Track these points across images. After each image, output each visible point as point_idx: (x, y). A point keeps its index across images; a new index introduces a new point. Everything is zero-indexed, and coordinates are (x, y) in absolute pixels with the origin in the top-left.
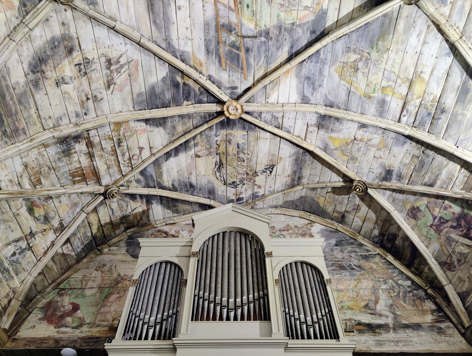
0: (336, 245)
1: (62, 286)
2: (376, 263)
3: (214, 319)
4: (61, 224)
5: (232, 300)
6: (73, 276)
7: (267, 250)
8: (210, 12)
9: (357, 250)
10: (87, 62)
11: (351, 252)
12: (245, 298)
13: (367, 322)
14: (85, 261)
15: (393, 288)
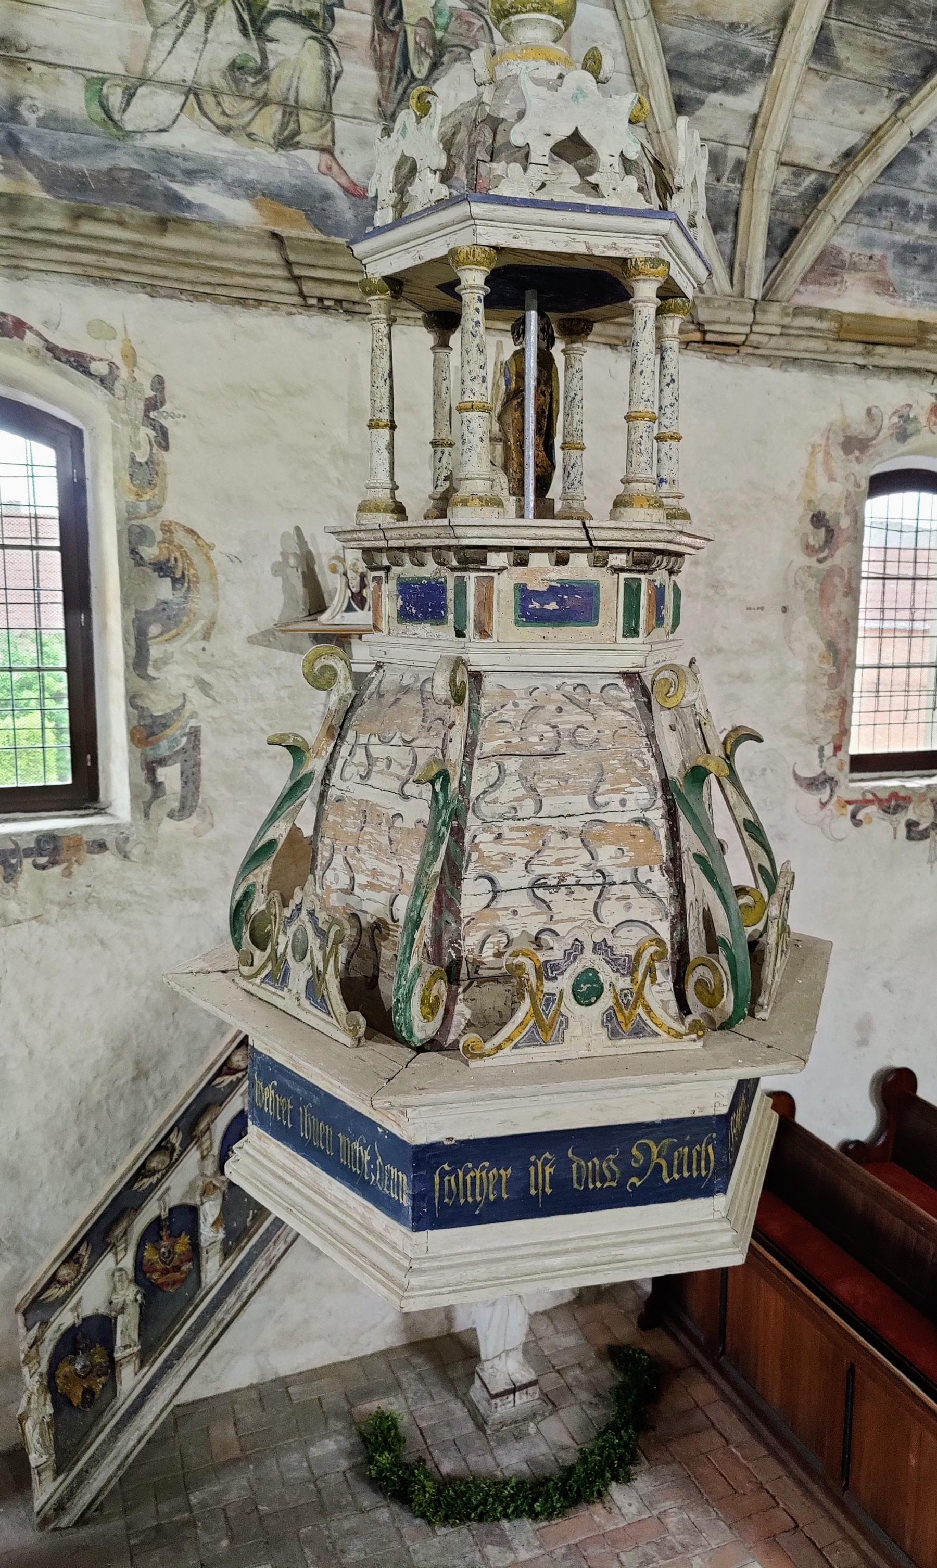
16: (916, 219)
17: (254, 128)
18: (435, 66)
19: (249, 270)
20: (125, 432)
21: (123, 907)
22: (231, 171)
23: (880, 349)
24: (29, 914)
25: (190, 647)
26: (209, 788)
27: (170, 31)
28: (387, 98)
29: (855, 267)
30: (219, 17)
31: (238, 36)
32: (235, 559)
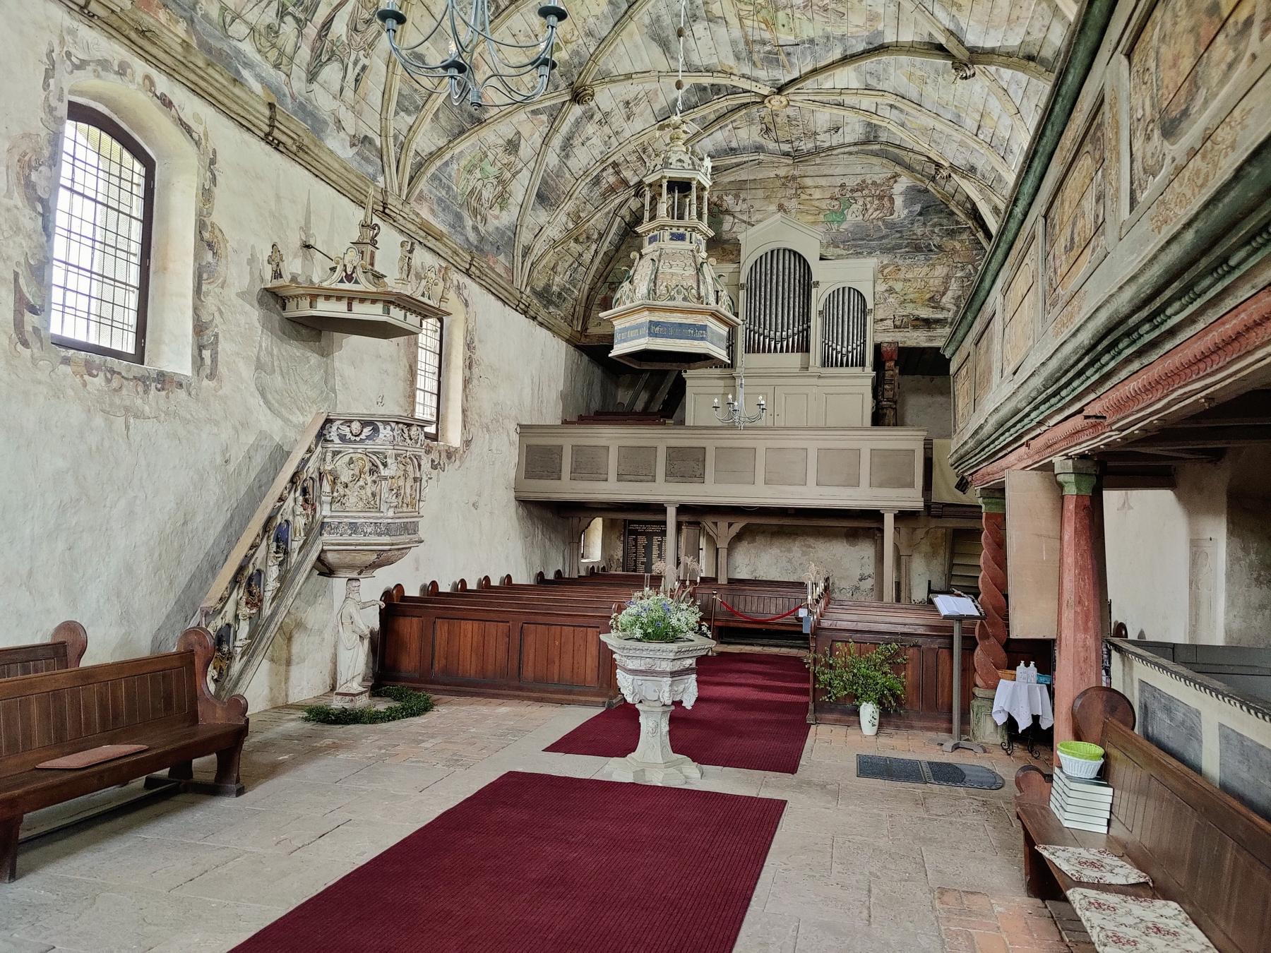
0: (920, 214)
1: (610, 279)
2: (962, 241)
3: (764, 351)
4: (599, 233)
5: (778, 334)
6: (617, 267)
7: (814, 279)
8: (736, 33)
9: (945, 221)
10: (606, 115)
11: (934, 225)
12: (790, 331)
13: (925, 317)
14: (623, 247)
15: (968, 276)
16: (443, 188)
17: (268, 55)
18: (329, 59)
19: (258, 115)
20: (202, 171)
21: (189, 422)
23: (430, 238)
24: (153, 415)
25: (216, 290)
29: (426, 200)
31: (274, 16)
32: (235, 251)
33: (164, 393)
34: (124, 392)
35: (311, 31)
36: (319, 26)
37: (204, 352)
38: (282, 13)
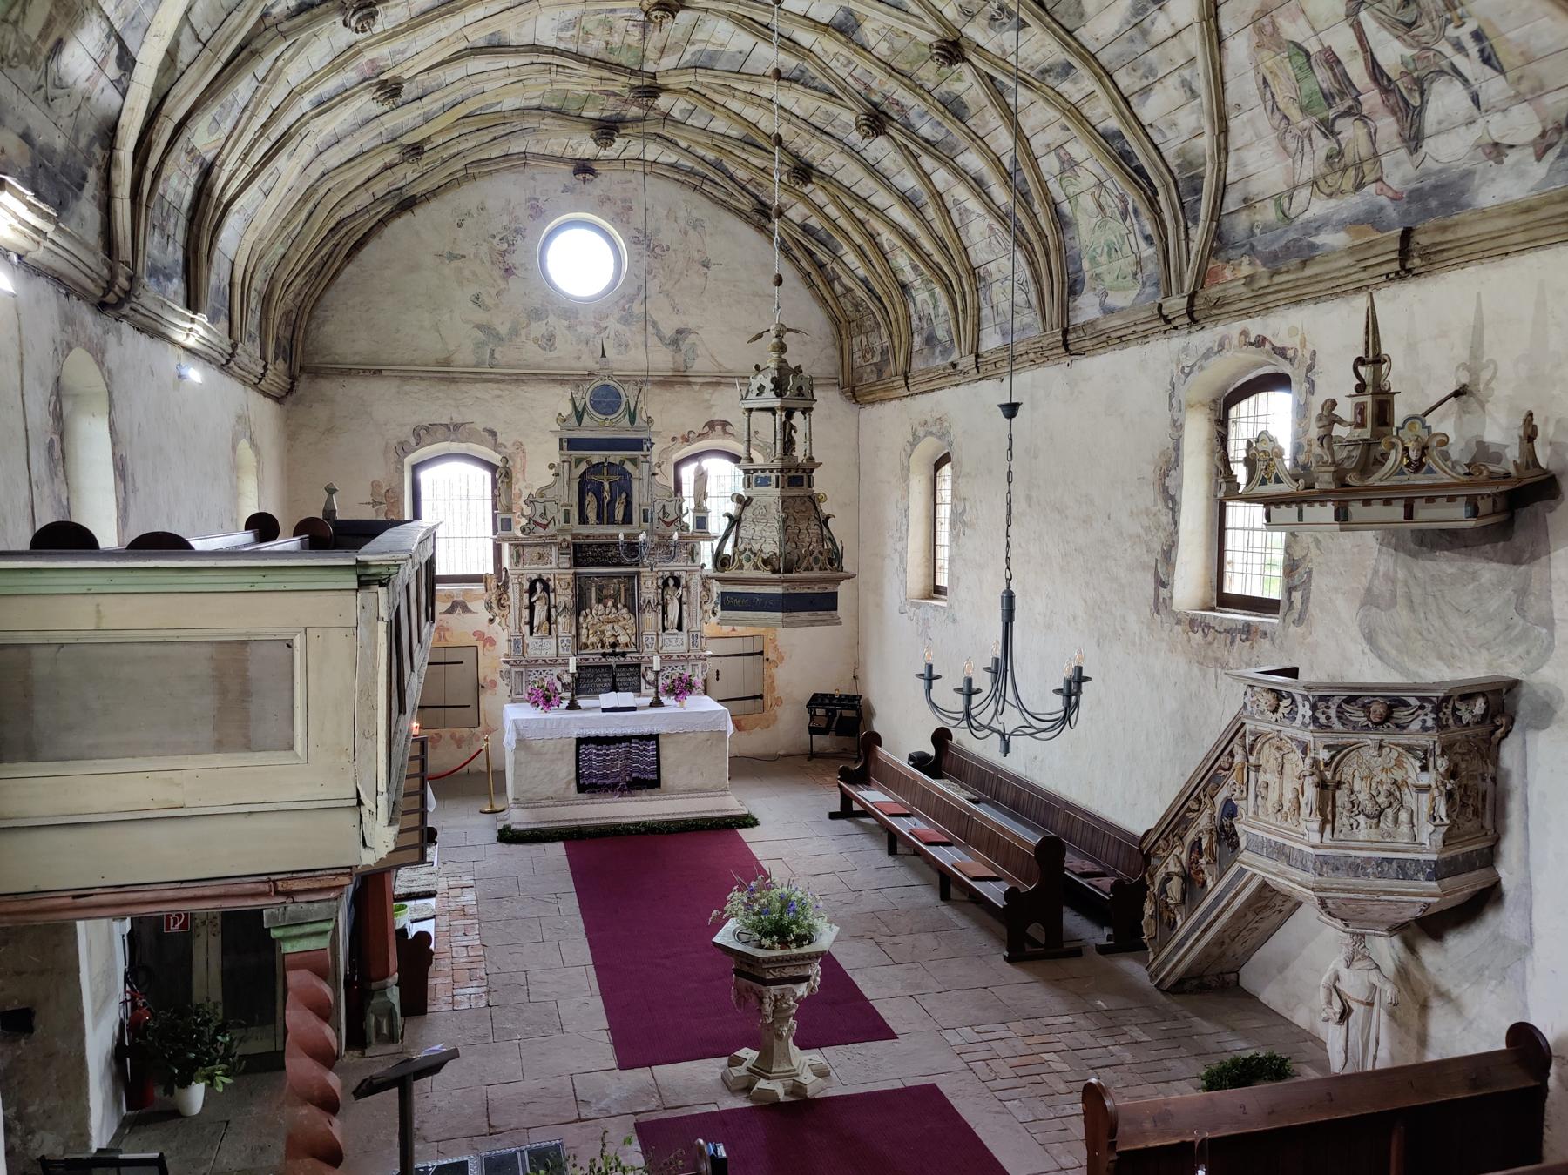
17: (1343, 187)
18: (1422, 94)
19: (1344, 273)
22: (1335, 218)
26: (1313, 609)
27: (1299, 156)
28: (1403, 129)
30: (1313, 136)
33: (1248, 644)
34: (1216, 645)
35: (1372, 98)
36: (1372, 86)
37: (1294, 594)
38: (1328, 128)
